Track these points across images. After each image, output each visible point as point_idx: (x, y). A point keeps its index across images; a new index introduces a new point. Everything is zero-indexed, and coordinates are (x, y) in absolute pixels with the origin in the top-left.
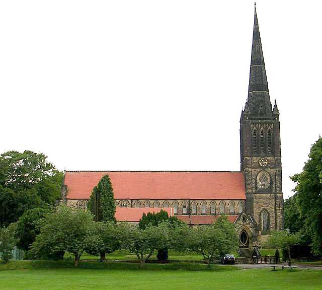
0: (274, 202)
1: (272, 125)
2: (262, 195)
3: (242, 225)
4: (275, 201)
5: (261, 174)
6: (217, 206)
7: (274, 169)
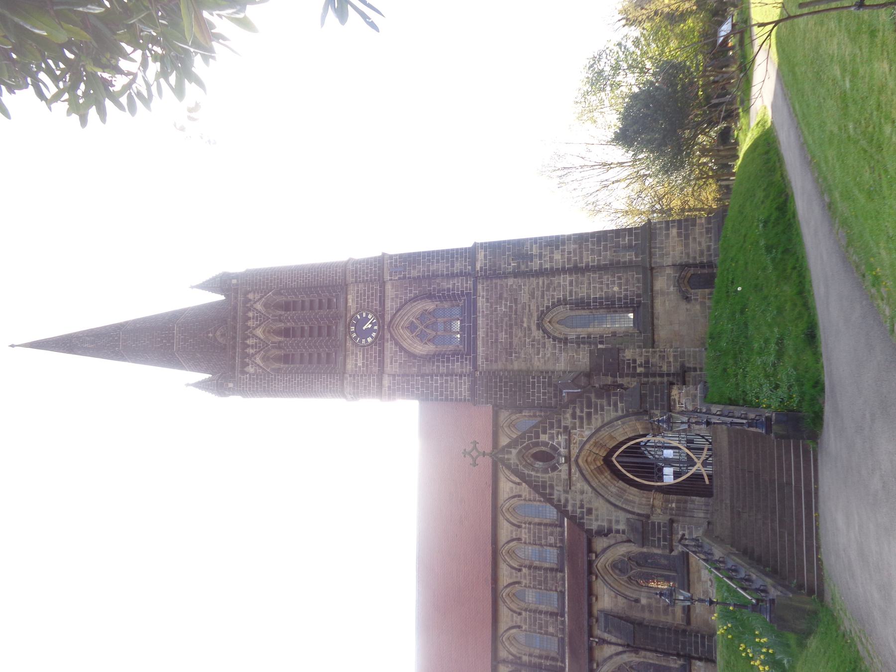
0: (510, 281)
1: (251, 296)
2: (481, 333)
3: (576, 475)
4: (506, 276)
5: (406, 334)
6: (524, 536)
7: (389, 287)
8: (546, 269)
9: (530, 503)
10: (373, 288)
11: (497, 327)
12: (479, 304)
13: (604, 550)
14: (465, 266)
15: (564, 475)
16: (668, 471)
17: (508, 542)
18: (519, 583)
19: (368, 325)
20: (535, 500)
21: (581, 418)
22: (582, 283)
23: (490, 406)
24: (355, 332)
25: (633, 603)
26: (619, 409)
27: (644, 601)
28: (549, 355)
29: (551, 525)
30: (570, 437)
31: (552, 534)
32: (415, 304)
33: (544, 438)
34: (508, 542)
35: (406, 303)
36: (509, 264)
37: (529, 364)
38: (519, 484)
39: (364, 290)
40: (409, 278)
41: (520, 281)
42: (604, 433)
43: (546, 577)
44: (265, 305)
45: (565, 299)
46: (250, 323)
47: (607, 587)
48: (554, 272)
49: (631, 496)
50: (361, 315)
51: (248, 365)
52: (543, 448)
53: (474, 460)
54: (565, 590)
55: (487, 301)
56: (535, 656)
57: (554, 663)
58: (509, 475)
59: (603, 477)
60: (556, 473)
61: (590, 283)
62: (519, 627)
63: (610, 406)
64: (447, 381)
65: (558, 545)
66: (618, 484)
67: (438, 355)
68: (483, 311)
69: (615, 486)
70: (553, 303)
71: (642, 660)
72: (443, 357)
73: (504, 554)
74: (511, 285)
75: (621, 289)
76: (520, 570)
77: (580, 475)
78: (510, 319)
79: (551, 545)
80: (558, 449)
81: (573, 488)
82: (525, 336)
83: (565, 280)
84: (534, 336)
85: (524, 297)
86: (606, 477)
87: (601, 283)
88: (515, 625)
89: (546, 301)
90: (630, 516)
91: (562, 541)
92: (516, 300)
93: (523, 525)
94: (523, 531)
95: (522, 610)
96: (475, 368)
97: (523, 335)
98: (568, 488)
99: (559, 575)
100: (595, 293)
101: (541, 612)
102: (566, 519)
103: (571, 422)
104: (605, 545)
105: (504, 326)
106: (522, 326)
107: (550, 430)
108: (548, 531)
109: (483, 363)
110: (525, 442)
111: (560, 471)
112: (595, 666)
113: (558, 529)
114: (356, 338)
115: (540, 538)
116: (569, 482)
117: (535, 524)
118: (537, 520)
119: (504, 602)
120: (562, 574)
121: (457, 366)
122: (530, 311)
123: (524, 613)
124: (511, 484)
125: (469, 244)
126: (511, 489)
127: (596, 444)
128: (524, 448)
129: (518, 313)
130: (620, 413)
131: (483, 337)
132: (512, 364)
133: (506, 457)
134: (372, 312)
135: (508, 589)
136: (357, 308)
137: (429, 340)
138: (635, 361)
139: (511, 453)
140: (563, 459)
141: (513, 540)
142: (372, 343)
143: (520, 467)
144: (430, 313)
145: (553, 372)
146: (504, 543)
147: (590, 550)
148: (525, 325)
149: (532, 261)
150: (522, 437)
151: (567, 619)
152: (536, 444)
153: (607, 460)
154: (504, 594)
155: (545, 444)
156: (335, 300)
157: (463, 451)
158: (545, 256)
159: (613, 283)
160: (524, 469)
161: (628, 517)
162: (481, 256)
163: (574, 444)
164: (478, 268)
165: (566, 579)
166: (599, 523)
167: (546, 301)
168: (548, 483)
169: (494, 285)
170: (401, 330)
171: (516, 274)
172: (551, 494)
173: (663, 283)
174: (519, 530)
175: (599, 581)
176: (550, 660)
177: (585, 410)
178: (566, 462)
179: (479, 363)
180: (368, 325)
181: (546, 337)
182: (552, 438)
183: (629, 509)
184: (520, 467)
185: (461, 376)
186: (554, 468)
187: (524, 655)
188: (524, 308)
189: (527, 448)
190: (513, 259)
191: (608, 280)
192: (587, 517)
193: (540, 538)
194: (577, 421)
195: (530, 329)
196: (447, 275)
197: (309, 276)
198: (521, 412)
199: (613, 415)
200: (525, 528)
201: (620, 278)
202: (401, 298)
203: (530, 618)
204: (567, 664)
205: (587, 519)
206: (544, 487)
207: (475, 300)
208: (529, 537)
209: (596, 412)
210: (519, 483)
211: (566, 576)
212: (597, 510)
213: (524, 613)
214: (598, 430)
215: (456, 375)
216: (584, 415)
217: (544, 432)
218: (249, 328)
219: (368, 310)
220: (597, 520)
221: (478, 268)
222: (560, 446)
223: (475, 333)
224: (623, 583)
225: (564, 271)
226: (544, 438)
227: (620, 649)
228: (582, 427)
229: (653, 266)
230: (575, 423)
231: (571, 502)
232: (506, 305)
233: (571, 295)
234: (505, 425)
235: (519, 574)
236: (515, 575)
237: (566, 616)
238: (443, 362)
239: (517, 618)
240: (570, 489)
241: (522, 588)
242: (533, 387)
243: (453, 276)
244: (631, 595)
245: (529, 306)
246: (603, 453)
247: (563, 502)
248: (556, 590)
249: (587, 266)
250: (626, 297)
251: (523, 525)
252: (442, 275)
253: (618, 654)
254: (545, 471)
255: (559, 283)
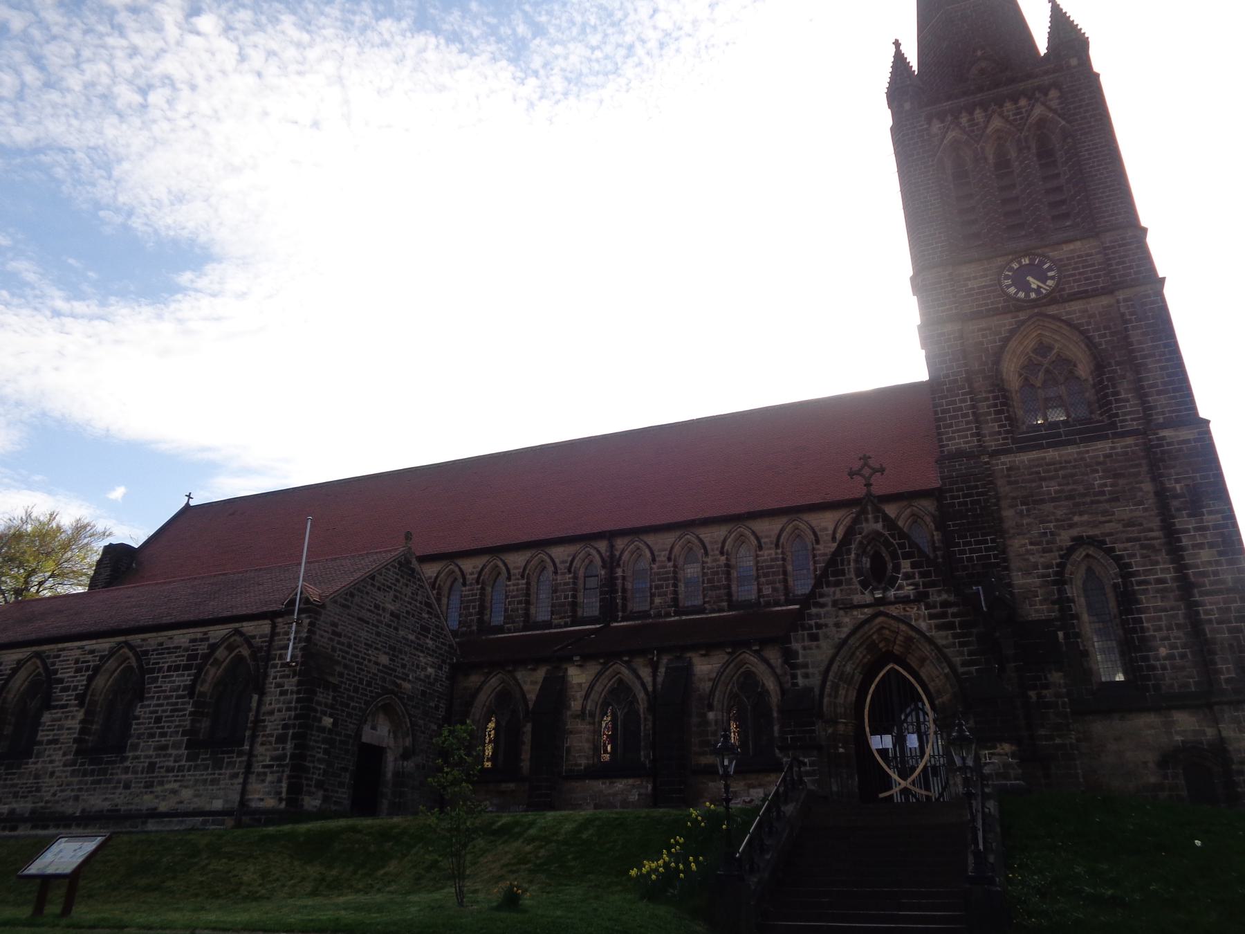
0: (1148, 487)
1: (1053, 93)
2: (1051, 454)
3: (860, 615)
7: (1105, 301)
8: (1179, 540)
9: (811, 557)
10: (1099, 277)
11: (1064, 477)
12: (1100, 445)
13: (766, 661)
14: (1163, 413)
15: (857, 599)
16: (887, 741)
17: (754, 533)
18: (706, 554)
19: (1034, 284)
20: (815, 562)
21: (944, 615)
22: (1163, 598)
23: (938, 484)
24: (1021, 266)
25: (706, 702)
26: (966, 669)
27: (711, 716)
28: (1033, 560)
29: (786, 588)
30: (914, 601)
31: (774, 589)
32: (1083, 346)
33: (906, 566)
34: (754, 533)
35: (1082, 333)
36: (1177, 481)
37: (1012, 531)
38: (834, 539)
39: (1093, 265)
40: (1126, 329)
41: (1150, 501)
42: (927, 650)
43: (719, 588)
44: (1042, 122)
45: (1133, 574)
46: (1008, 105)
47: (723, 666)
48: (1175, 551)
49: (844, 692)
50: (1050, 269)
51: (942, 121)
52: (890, 566)
53: (858, 473)
54: (707, 614)
55: (1106, 456)
56: (623, 584)
57: (620, 607)
58: (844, 523)
59: (865, 653)
60: (859, 587)
61: (1165, 610)
62: (654, 560)
63: (968, 656)
64: (966, 415)
65: (762, 600)
66: (858, 674)
67: (1004, 397)
68: (1088, 452)
69: (855, 669)
70: (1121, 557)
71: (642, 716)
72: (1003, 404)
73: (739, 530)
74: (1141, 490)
75: (1165, 658)
76: (722, 553)
77: (861, 621)
78: (1085, 495)
79: (760, 590)
80: (893, 587)
81: (841, 613)
82: (1057, 520)
83: (1164, 570)
84: (1059, 535)
85: (1124, 511)
86: (864, 657)
87: (1169, 628)
88: (656, 553)
89: (1121, 546)
90: (817, 691)
91: (768, 604)
92: (1117, 499)
93: (779, 551)
94: (773, 552)
95: (675, 561)
96: (995, 454)
97: (1059, 517)
98: (841, 606)
99: (725, 604)
100: (1148, 620)
101: (675, 585)
102: (797, 607)
103: (936, 602)
104: (772, 661)
105: (1070, 487)
106: (1074, 514)
107: (920, 573)
108: (778, 585)
109: (1003, 464)
110: (895, 540)
111: (863, 593)
112: (626, 659)
113: (782, 598)
114: (1011, 269)
115: (766, 575)
116: (849, 607)
117: (784, 566)
118: (790, 568)
119: (680, 538)
120: (726, 608)
121: (993, 427)
122: (1101, 522)
123: (671, 564)
124: (831, 527)
125: (1203, 414)
126: (826, 529)
127: (909, 639)
128: (886, 539)
129: (1094, 506)
130: (961, 670)
131: (1044, 458)
132: (1011, 506)
133: (870, 516)
134: (1057, 285)
135: (696, 541)
136: (1061, 260)
137: (1026, 379)
138: (1046, 687)
139: (877, 522)
140: (881, 596)
141: (758, 538)
142: (1007, 295)
143: (859, 537)
144: (1071, 372)
145: (1007, 568)
146: (753, 528)
147: (764, 643)
148: (1076, 519)
149: (1190, 515)
150: (902, 535)
151: (673, 619)
152: (894, 556)
153: (889, 657)
154: (688, 536)
155: (897, 568)
156: (1068, 224)
157: (868, 455)
158: (1204, 536)
159: (1173, 647)
160: (856, 543)
161: (815, 690)
162: (1185, 434)
163: (904, 609)
164: (1163, 433)
165: (721, 614)
166: (801, 651)
167: (1121, 546)
168: (843, 578)
169: (1137, 462)
170: (1035, 334)
171: (1162, 496)
172: (828, 586)
173: (1185, 724)
174: (773, 546)
175: (726, 657)
176: (623, 603)
177: (957, 620)
178: (875, 599)
179: (1003, 459)
180: (1034, 284)
181: (1062, 553)
182: (907, 576)
183: (827, 690)
184: (859, 537)
185: (978, 434)
186: (864, 585)
187: (623, 570)
188: (1105, 513)
189: (887, 544)
190: (1187, 485)
191: (1175, 638)
192: (806, 635)
193: (766, 575)
194: (939, 610)
195: (1071, 526)
196: (1142, 387)
197: (1102, 174)
198: (937, 529)
199: (957, 660)
200: (777, 554)
201: (1183, 656)
202: (1089, 323)
203: (667, 573)
204: (622, 624)
205: (804, 635)
206: (835, 574)
207: (1106, 437)
208: (765, 561)
209: (955, 636)
210: (835, 538)
211: (725, 614)
212: (818, 647)
213: (671, 564)
214: (930, 641)
215: (977, 428)
216: (950, 619)
217: (913, 566)
218: (1001, 106)
219: (1060, 279)
220: (804, 648)
221: (1163, 433)
222: (898, 589)
223: (1050, 446)
224: (729, 688)
225: (1181, 567)
226: (906, 566)
227: (650, 688)
228: (931, 617)
229: (1216, 708)
230: (935, 607)
231: (822, 611)
232: (1106, 486)
233: (1140, 583)
234: (914, 508)
235: (717, 552)
236: (716, 546)
237: (677, 618)
238: (995, 405)
239: (664, 556)
240: (840, 609)
241: (700, 556)
242: (977, 542)
243: (1142, 396)
244: (716, 699)
245: (1110, 521)
246: (897, 649)
247: (822, 600)
248: (705, 603)
249: (1197, 604)
250: (1153, 668)
251: (779, 551)
252: (1140, 380)
253: (643, 685)
254: (859, 572)
255: (1157, 563)
